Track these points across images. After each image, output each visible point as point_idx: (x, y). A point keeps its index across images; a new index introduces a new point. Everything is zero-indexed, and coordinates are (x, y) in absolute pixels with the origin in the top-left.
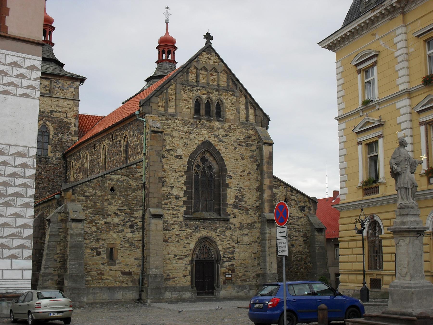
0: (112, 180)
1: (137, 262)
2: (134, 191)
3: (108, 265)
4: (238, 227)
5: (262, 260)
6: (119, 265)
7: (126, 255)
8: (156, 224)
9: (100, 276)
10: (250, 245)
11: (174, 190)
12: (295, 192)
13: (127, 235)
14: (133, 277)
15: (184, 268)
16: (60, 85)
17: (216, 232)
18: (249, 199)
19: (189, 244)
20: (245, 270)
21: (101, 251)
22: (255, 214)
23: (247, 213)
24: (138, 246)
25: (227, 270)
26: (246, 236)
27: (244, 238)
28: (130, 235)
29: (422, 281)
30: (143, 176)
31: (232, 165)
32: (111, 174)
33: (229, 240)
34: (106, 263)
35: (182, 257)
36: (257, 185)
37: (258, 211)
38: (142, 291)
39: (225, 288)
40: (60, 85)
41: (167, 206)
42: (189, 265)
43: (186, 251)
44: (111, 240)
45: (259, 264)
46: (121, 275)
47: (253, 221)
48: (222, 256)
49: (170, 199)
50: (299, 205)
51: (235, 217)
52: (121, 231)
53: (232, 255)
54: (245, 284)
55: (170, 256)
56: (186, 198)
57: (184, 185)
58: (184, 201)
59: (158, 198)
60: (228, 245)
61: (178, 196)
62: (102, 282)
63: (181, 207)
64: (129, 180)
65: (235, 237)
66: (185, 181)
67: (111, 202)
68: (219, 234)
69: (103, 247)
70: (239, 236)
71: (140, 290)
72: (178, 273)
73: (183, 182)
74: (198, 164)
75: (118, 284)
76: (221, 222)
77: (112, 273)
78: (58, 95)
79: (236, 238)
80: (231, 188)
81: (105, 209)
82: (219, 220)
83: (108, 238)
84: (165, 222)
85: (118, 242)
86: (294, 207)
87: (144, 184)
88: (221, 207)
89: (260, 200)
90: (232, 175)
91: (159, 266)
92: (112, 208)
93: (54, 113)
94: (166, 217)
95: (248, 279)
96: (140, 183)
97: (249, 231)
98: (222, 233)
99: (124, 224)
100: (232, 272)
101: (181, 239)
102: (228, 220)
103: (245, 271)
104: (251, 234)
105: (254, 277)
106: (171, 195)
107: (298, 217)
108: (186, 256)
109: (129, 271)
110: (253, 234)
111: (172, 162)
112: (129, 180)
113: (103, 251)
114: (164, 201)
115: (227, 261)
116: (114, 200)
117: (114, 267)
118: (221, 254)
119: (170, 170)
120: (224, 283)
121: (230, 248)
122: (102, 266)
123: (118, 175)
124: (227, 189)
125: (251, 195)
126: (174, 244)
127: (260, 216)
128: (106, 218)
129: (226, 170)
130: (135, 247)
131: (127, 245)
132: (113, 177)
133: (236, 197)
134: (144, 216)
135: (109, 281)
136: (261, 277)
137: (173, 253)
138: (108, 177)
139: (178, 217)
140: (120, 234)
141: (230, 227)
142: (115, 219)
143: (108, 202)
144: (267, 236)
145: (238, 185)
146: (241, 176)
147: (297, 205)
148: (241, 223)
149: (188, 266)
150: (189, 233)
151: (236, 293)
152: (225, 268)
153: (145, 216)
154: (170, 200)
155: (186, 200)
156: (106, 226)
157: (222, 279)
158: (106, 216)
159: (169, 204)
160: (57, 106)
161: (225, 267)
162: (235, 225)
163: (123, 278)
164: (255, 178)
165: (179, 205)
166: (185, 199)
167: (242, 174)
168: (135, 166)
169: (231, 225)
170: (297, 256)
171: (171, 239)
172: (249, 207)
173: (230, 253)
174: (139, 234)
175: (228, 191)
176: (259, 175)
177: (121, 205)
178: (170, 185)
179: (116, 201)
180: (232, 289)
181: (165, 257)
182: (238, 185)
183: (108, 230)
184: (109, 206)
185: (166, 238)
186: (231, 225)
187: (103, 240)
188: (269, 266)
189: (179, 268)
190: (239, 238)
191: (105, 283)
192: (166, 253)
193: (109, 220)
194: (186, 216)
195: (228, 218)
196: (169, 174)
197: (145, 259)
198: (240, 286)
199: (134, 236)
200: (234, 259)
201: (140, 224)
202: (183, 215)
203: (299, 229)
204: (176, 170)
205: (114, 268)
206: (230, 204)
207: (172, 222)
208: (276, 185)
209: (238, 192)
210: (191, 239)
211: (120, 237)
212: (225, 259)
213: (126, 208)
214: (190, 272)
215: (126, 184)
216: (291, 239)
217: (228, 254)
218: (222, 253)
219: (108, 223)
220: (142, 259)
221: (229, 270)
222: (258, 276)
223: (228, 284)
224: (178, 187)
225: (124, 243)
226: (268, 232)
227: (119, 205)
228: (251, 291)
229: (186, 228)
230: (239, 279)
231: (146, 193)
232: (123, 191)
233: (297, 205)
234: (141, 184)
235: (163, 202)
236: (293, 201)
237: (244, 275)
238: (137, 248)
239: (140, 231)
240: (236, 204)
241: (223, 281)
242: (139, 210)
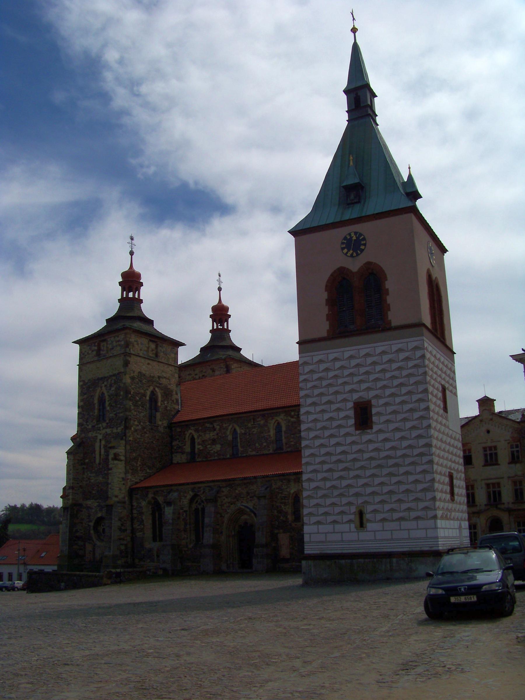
16: (164, 349)
40: (164, 349)
78: (163, 361)
93: (161, 379)
160: (163, 371)
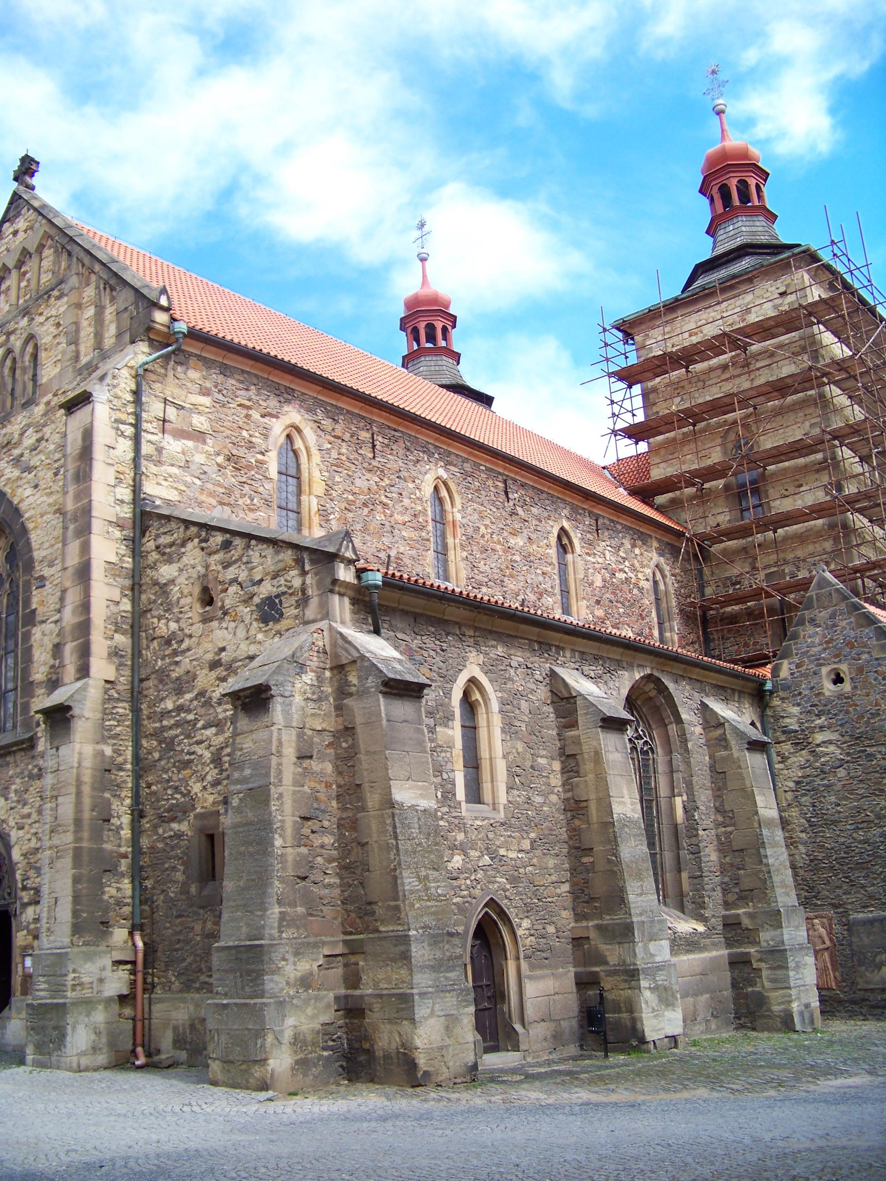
17: (7, 799)
48: (20, 885)
216: (222, 771)
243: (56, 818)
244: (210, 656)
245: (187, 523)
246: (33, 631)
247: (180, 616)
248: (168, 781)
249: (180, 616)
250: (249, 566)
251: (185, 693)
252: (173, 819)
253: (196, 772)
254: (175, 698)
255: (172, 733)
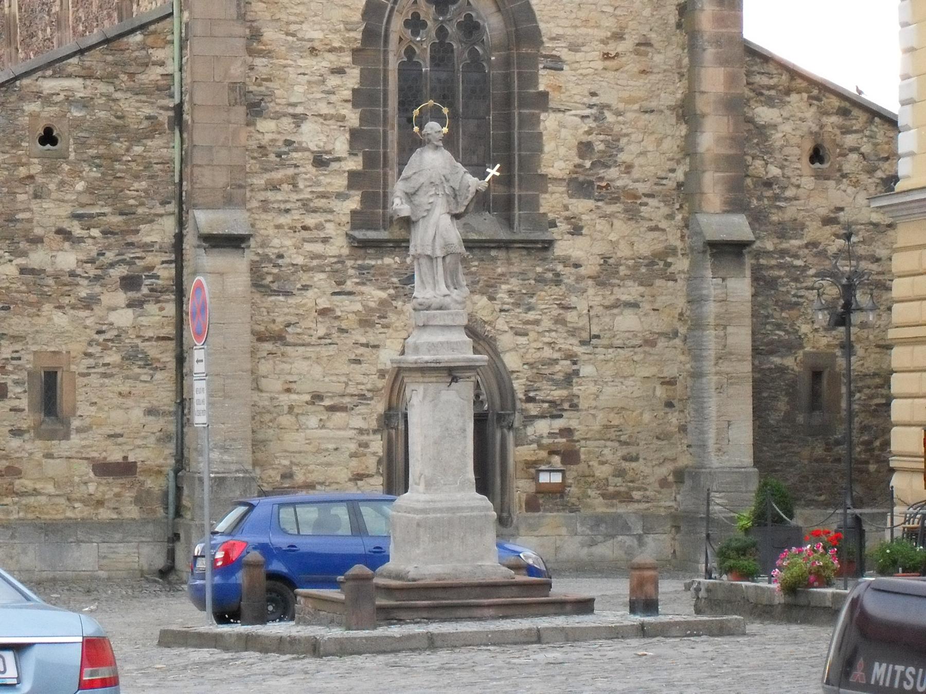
0: (47, 100)
1: (156, 424)
2: (137, 138)
3: (39, 436)
4: (594, 274)
5: (692, 413)
6: (83, 435)
7: (111, 395)
8: (221, 274)
9: (8, 479)
10: (647, 349)
11: (306, 127)
12: (863, 117)
13: (114, 317)
14: (142, 484)
15: (353, 447)
17: (492, 298)
18: (643, 153)
19: (376, 347)
20: (623, 451)
21: (10, 383)
22: (670, 217)
23: (632, 215)
24: (158, 360)
25: (543, 454)
26: (628, 312)
27: (619, 318)
28: (124, 318)
29: (459, 496)
30: (172, 75)
31: (562, 14)
32: (40, 73)
33: (550, 331)
34: (28, 431)
35: (347, 400)
36: (679, 96)
37: (681, 206)
38: (176, 537)
39: (532, 528)
41: (280, 196)
42: (375, 432)
43: (360, 378)
44: (45, 337)
45: (683, 429)
46: (92, 474)
47: (659, 247)
48: (520, 395)
49: (290, 166)
50: (879, 174)
51: (576, 231)
52: (89, 303)
53: (564, 393)
54: (622, 509)
55: (294, 397)
56: (360, 159)
57: (349, 105)
58: (352, 175)
59: (231, 168)
60: (546, 348)
61: (327, 153)
62: (15, 503)
63: (340, 196)
64: (118, 95)
65: (580, 316)
66: (354, 90)
67: (43, 186)
68: (506, 307)
69: (16, 367)
70: (598, 310)
71: (170, 535)
72: (329, 464)
73: (348, 94)
74: (416, 16)
75: (80, 511)
76: (514, 256)
77: (54, 467)
79: (583, 322)
80: (559, 111)
81: (20, 216)
82: (505, 245)
83: (37, 332)
84: (270, 261)
85: (77, 348)
86: (856, 184)
87: (179, 109)
88: (516, 192)
89: (688, 160)
90: (565, 54)
91: (234, 440)
92: (48, 212)
94: (276, 242)
95: (639, 489)
96: (162, 108)
97: (642, 289)
98: (521, 301)
99: (99, 272)
100: (563, 462)
101: (342, 330)
102: (548, 245)
103: (625, 459)
104: (652, 302)
105: (663, 483)
106: (296, 150)
107: (876, 225)
108: (362, 397)
109: (125, 458)
110: (660, 302)
111: (295, 14)
112: (118, 95)
113: (17, 383)
114: (267, 176)
115: (542, 417)
116: (56, 180)
117: (64, 444)
118: (519, 386)
119: (291, 48)
120: (532, 505)
121: (556, 361)
122: (15, 443)
123: (69, 76)
124: (543, 116)
125: (653, 138)
126: (309, 349)
127: (687, 226)
128: (24, 254)
129: (533, 36)
130: (148, 363)
131: (113, 357)
132: (49, 85)
133: (585, 148)
134: (179, 238)
135: (43, 499)
136: (688, 483)
137: (307, 387)
138: (27, 86)
139: (325, 240)
140: (83, 314)
141: (558, 275)
142: (60, 253)
143: (30, 189)
144: (711, 309)
145: (593, 94)
146: (606, 56)
147: (871, 171)
148: (606, 259)
149: (372, 437)
150: (372, 305)
151: (583, 546)
152: (534, 446)
153: (185, 240)
154: (291, 171)
155: (360, 168)
156: (27, 285)
157: (521, 488)
158: (23, 245)
159: (285, 187)
161: (532, 442)
162: (577, 266)
163: (101, 488)
164: (672, 62)
165: (329, 189)
166: (355, 164)
167: (612, 48)
168: (138, 37)
169: (560, 268)
170: (867, 391)
171: (299, 330)
172: (642, 188)
173: (557, 384)
174: (164, 313)
175: (549, 122)
176: (683, 49)
177: (85, 199)
178: (291, 110)
179: (62, 183)
180: (564, 531)
181: (276, 403)
182: (593, 94)
183: (33, 298)
184: (35, 205)
185: (275, 328)
186: (560, 268)
187: (16, 338)
188: (718, 433)
189: (331, 446)
190: (595, 320)
191: (27, 507)
192: (278, 385)
193: (37, 258)
194: (359, 234)
195: (546, 236)
196: (283, 62)
197: (186, 411)
198: (598, 520)
199: (144, 321)
200: (574, 407)
201: (166, 273)
202: (347, 228)
203: (880, 277)
204: (316, 44)
205: (61, 447)
206: (555, 179)
207: (300, 260)
208: (770, 88)
209: (594, 125)
210: (384, 326)
211: (86, 327)
212: (533, 408)
213: (106, 210)
214: (379, 462)
215: (102, 114)
217: (545, 385)
218: (523, 381)
219: (32, 271)
220: (175, 413)
221: (552, 453)
222: (680, 475)
223: (545, 510)
224: (325, 117)
225: (99, 349)
226: (713, 292)
227: (76, 200)
228: (650, 539)
229: (364, 284)
230: (598, 488)
231: (185, 146)
232: (92, 141)
233: (871, 171)
234: (167, 109)
235: (259, 181)
236: (854, 157)
237: (620, 473)
238: (156, 368)
239: (167, 301)
240: (581, 178)
241: (524, 497)
242: (161, 215)
243: (725, 346)
244: (823, 212)
245: (793, 73)
246: (542, 117)
247: (785, 163)
248: (767, 317)
249: (785, 163)
250: (874, 141)
251: (791, 238)
252: (772, 353)
253: (804, 314)
254: (776, 241)
255: (776, 273)
